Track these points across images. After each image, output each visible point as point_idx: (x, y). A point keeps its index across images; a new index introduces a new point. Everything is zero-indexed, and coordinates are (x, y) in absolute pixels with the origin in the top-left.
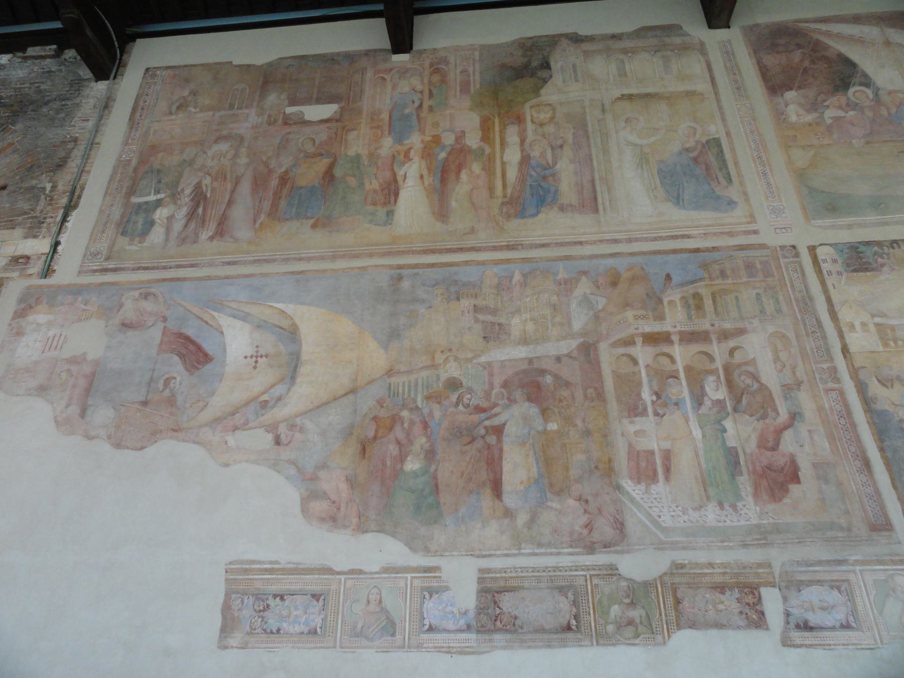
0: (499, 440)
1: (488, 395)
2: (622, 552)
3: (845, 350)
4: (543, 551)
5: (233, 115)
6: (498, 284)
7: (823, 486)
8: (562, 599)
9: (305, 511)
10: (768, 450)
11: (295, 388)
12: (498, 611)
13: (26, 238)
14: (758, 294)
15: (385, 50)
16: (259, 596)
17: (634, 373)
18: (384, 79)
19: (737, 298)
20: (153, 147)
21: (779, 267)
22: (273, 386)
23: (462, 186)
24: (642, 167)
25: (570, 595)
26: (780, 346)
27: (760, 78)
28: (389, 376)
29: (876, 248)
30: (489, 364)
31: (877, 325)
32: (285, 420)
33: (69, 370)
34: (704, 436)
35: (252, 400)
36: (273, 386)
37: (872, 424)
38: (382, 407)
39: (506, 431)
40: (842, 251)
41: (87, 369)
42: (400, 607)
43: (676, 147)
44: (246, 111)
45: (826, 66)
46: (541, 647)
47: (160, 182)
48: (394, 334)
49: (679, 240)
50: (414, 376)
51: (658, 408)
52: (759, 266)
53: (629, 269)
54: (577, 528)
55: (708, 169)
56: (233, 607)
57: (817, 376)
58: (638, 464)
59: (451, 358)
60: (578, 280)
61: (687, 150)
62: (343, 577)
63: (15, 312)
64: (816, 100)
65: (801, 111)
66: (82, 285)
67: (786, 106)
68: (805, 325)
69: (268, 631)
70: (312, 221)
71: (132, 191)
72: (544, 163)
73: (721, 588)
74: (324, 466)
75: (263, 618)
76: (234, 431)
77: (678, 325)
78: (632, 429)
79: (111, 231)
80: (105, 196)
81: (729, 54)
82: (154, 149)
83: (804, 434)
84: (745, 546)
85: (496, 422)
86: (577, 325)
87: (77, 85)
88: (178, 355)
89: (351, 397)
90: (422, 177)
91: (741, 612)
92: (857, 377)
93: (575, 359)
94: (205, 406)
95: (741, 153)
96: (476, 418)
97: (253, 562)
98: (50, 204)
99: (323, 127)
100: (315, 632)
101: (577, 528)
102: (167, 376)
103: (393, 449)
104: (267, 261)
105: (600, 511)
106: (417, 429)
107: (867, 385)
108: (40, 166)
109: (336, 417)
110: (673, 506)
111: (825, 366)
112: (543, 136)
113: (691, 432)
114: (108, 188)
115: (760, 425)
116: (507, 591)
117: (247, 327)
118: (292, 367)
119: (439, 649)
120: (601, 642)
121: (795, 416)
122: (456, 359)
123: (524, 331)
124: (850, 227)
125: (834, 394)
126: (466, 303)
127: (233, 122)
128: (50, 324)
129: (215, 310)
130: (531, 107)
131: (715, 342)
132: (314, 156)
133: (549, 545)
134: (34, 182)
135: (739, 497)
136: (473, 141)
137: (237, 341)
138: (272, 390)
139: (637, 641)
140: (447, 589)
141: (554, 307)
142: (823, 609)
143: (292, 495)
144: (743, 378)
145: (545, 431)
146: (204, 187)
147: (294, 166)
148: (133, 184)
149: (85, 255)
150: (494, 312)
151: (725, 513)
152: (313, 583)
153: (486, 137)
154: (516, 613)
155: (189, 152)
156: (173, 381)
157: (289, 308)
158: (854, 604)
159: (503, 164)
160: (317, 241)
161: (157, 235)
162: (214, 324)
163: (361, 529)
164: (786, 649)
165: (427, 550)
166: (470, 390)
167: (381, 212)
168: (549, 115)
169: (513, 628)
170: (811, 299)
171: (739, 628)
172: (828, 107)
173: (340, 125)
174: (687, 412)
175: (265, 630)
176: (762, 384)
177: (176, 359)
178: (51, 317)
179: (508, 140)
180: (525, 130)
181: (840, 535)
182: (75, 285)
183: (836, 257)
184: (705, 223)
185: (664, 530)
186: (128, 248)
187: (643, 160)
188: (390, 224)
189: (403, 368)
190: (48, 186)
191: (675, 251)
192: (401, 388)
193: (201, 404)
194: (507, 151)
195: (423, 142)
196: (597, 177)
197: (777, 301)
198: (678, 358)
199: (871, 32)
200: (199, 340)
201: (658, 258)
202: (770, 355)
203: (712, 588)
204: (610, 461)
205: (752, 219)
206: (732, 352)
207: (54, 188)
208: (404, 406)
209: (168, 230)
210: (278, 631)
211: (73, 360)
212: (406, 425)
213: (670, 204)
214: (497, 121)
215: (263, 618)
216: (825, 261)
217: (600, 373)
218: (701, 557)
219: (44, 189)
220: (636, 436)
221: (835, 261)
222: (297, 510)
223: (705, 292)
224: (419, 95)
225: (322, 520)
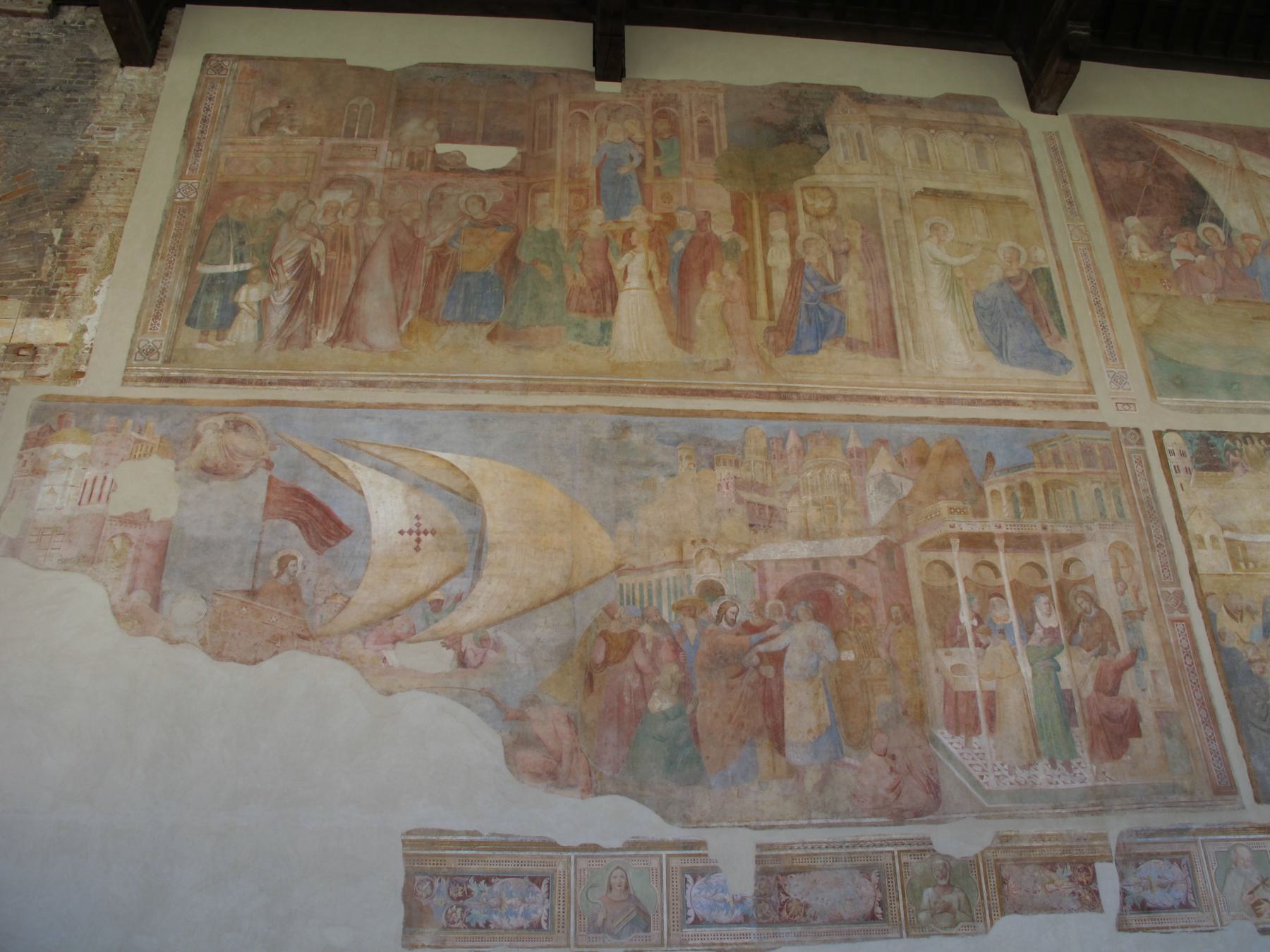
0: (779, 673)
1: (760, 608)
2: (938, 822)
3: (1193, 569)
4: (839, 821)
5: (354, 146)
6: (769, 448)
7: (1167, 741)
8: (863, 881)
9: (510, 760)
11: (481, 584)
12: (784, 898)
13: (28, 315)
14: (1097, 491)
15: (584, 72)
16: (455, 879)
17: (949, 587)
18: (584, 117)
20: (226, 185)
21: (1121, 456)
22: (447, 579)
23: (710, 298)
24: (954, 298)
25: (874, 876)
26: (1122, 562)
28: (620, 574)
29: (1228, 442)
30: (760, 563)
31: (1228, 540)
32: (471, 631)
33: (124, 535)
34: (1034, 675)
35: (417, 599)
36: (447, 579)
37: (1220, 665)
38: (613, 618)
39: (787, 659)
40: (1191, 441)
41: (155, 535)
42: (652, 893)
43: (996, 274)
44: (373, 142)
46: (840, 941)
47: (242, 243)
48: (623, 512)
49: (1002, 408)
50: (656, 576)
51: (980, 636)
52: (1098, 452)
53: (941, 443)
54: (881, 791)
55: (1035, 311)
56: (420, 893)
57: (1163, 603)
58: (956, 708)
59: (706, 553)
60: (875, 452)
61: (1010, 280)
62: (572, 855)
63: (27, 437)
65: (1145, 247)
66: (131, 401)
67: (1128, 236)
68: (1150, 536)
69: (473, 924)
70: (487, 329)
71: (198, 254)
72: (824, 274)
73: (1051, 864)
74: (534, 701)
75: (464, 908)
76: (394, 642)
77: (1003, 525)
78: (948, 662)
79: (169, 317)
80: (154, 258)
82: (227, 189)
83: (1148, 675)
84: (1080, 813)
85: (775, 646)
86: (876, 516)
87: (89, 68)
88: (295, 522)
89: (566, 601)
90: (650, 275)
91: (1073, 893)
92: (1205, 603)
93: (873, 562)
94: (347, 602)
95: (1075, 293)
98: (63, 264)
99: (495, 181)
100: (539, 927)
101: (881, 791)
102: (281, 554)
104: (423, 385)
105: (910, 769)
106: (665, 653)
107: (1215, 615)
108: (38, 200)
109: (546, 630)
110: (998, 763)
111: (1171, 590)
112: (822, 234)
113: (1019, 669)
114: (157, 246)
115: (1097, 663)
116: (795, 873)
117: (400, 487)
118: (475, 552)
120: (913, 932)
121: (1137, 653)
122: (713, 554)
124: (1199, 410)
125: (1180, 626)
127: (353, 158)
128: (87, 460)
129: (346, 455)
130: (803, 189)
131: (1047, 552)
132: (485, 225)
134: (32, 224)
135: (1073, 753)
136: (722, 229)
137: (385, 507)
138: (447, 585)
139: (954, 931)
140: (715, 870)
142: (1162, 886)
144: (1079, 600)
145: (839, 663)
146: (314, 258)
147: (455, 237)
148: (199, 243)
149: (131, 352)
150: (762, 488)
151: (1057, 772)
152: (531, 861)
153: (741, 226)
155: (287, 200)
156: (292, 562)
158: (1195, 880)
159: (767, 269)
160: (498, 360)
161: (244, 330)
162: (347, 478)
163: (591, 790)
164: (1121, 933)
165: (686, 821)
166: (734, 601)
167: (593, 324)
168: (828, 204)
169: (803, 920)
170: (1156, 501)
171: (1070, 911)
172: (1175, 245)
173: (524, 180)
174: (1014, 643)
175: (468, 924)
176: (1101, 610)
177: (293, 528)
178: (86, 449)
179: (773, 233)
180: (795, 222)
181: (1182, 799)
182: (120, 400)
183: (1185, 448)
184: (1035, 386)
185: (987, 794)
186: (199, 346)
187: (954, 285)
188: (607, 344)
189: (639, 564)
190: (57, 234)
191: (998, 422)
193: (339, 600)
194: (772, 250)
195: (649, 221)
196: (895, 305)
197: (1119, 502)
199: (1222, 150)
200: (326, 502)
201: (977, 428)
202: (1109, 572)
203: (1041, 865)
204: (922, 705)
205: (1090, 387)
206: (1067, 565)
207: (66, 236)
208: (644, 618)
209: (262, 322)
210: (487, 925)
211: (128, 520)
212: (649, 646)
213: (991, 354)
214: (755, 203)
215: (464, 908)
216: (1172, 453)
218: (1030, 828)
219: (50, 237)
221: (1183, 454)
222: (499, 759)
223: (1035, 483)
224: (640, 149)
225: (537, 776)
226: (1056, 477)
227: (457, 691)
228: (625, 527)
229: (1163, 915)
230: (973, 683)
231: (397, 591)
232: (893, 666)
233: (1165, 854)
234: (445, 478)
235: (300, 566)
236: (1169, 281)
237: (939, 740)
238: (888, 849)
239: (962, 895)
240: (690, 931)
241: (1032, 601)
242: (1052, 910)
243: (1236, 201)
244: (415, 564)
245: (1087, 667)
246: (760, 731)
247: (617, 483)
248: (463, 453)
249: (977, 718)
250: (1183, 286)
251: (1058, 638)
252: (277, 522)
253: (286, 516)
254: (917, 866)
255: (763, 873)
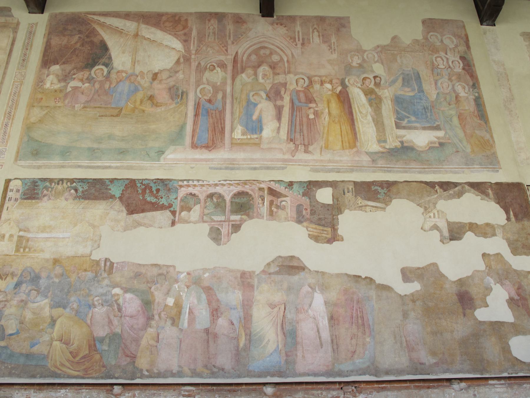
27: (42, 54)
29: (48, 184)
45: (89, 48)
64: (69, 73)
65: (55, 81)
67: (47, 76)
81: (31, 34)
124: (39, 167)
216: (12, 190)
236: (60, 98)
243: (123, 53)
250: (67, 101)
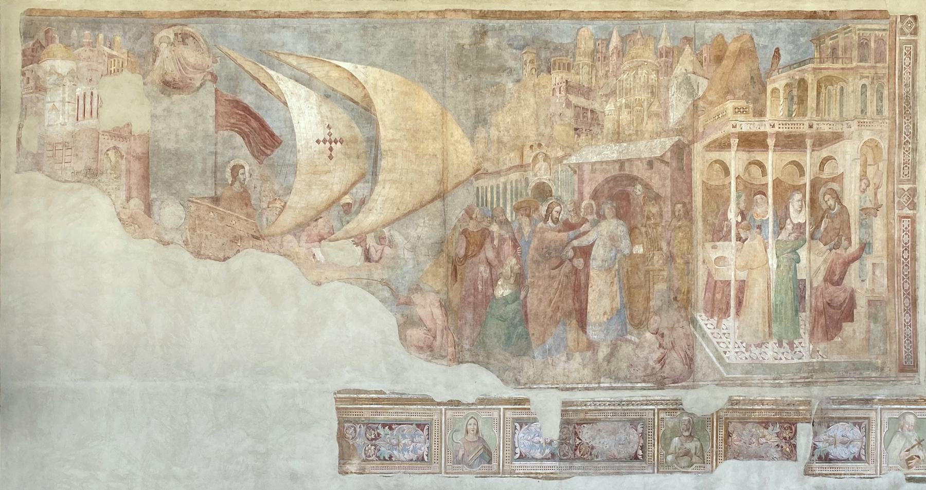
0: (586, 265)
4: (619, 385)
6: (593, 51)
7: (872, 325)
9: (403, 338)
10: (833, 284)
11: (378, 189)
12: (578, 441)
14: (864, 86)
16: (370, 425)
19: (842, 89)
21: (893, 49)
22: (353, 184)
28: (477, 179)
30: (580, 166)
32: (372, 231)
34: (778, 266)
35: (333, 202)
36: (353, 184)
38: (471, 218)
39: (593, 253)
42: (494, 437)
48: (480, 119)
50: (503, 179)
52: (872, 44)
54: (651, 363)
57: (897, 200)
58: (714, 295)
59: (540, 157)
60: (681, 51)
68: (900, 133)
73: (765, 423)
74: (417, 288)
75: (375, 445)
76: (320, 241)
77: (776, 123)
78: (714, 255)
83: (869, 267)
84: (793, 384)
85: (584, 241)
86: (675, 116)
88: (240, 134)
89: (438, 204)
94: (284, 207)
96: (564, 236)
97: (359, 391)
100: (423, 460)
102: (232, 163)
103: (483, 270)
106: (507, 248)
109: (424, 230)
110: (739, 342)
111: (906, 187)
113: (767, 262)
117: (314, 97)
119: (528, 475)
121: (865, 247)
122: (546, 157)
123: (618, 122)
125: (906, 222)
126: (557, 77)
131: (809, 151)
133: (626, 379)
137: (305, 118)
138: (354, 190)
140: (535, 420)
141: (653, 91)
142: (843, 443)
143: (388, 321)
150: (587, 92)
151: (782, 350)
152: (417, 413)
154: (593, 443)
156: (241, 171)
157: (360, 71)
162: (274, 90)
165: (517, 382)
174: (767, 238)
176: (843, 207)
177: (239, 139)
185: (727, 366)
192: (489, 195)
193: (278, 204)
197: (881, 98)
198: (770, 170)
200: (261, 113)
201: (771, 25)
203: (758, 423)
204: (688, 292)
210: (390, 457)
212: (496, 242)
217: (691, 183)
218: (753, 393)
220: (715, 263)
222: (395, 338)
225: (420, 349)
226: (830, 73)
227: (365, 281)
228: (482, 133)
229: (840, 465)
230: (730, 273)
231: (319, 197)
232: (671, 258)
233: (851, 418)
234: (345, 88)
235: (247, 174)
237: (697, 321)
238: (651, 407)
239: (698, 443)
240: (517, 464)
241: (789, 199)
242: (760, 457)
244: (330, 172)
245: (822, 259)
246: (570, 313)
247: (477, 90)
248: (360, 62)
249: (728, 304)
251: (804, 233)
252: (226, 133)
253: (232, 127)
254: (670, 421)
255: (565, 423)
